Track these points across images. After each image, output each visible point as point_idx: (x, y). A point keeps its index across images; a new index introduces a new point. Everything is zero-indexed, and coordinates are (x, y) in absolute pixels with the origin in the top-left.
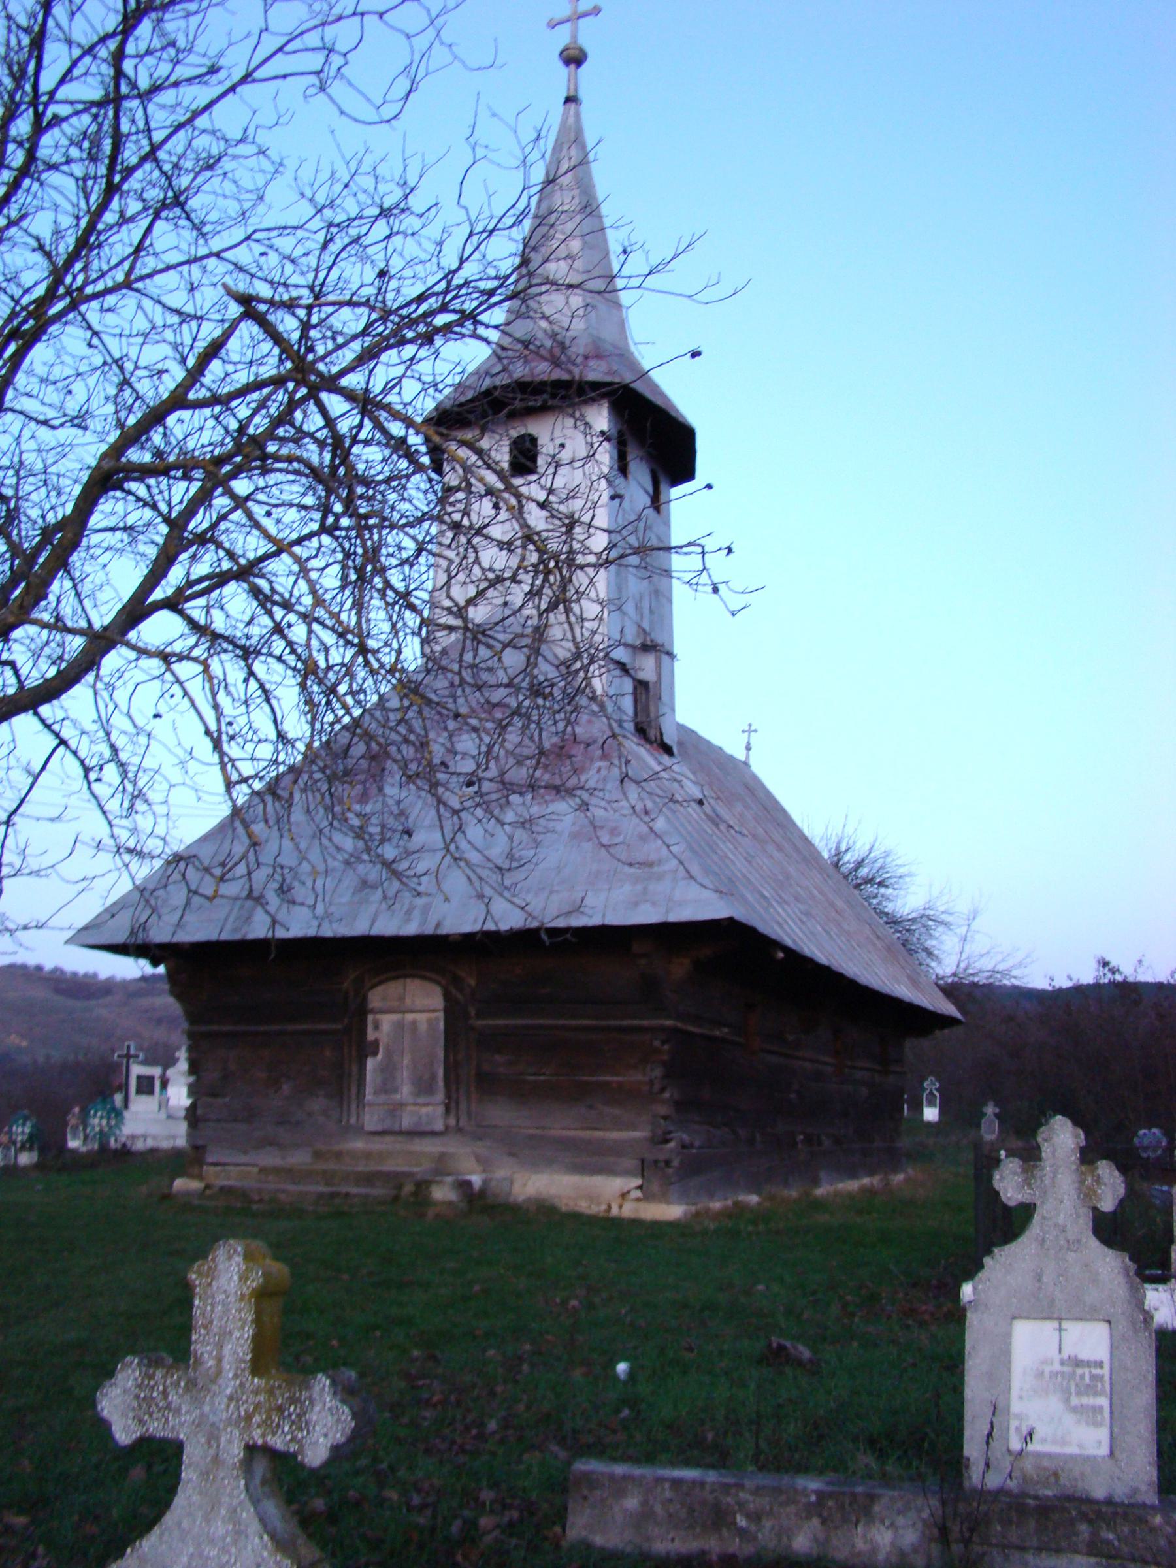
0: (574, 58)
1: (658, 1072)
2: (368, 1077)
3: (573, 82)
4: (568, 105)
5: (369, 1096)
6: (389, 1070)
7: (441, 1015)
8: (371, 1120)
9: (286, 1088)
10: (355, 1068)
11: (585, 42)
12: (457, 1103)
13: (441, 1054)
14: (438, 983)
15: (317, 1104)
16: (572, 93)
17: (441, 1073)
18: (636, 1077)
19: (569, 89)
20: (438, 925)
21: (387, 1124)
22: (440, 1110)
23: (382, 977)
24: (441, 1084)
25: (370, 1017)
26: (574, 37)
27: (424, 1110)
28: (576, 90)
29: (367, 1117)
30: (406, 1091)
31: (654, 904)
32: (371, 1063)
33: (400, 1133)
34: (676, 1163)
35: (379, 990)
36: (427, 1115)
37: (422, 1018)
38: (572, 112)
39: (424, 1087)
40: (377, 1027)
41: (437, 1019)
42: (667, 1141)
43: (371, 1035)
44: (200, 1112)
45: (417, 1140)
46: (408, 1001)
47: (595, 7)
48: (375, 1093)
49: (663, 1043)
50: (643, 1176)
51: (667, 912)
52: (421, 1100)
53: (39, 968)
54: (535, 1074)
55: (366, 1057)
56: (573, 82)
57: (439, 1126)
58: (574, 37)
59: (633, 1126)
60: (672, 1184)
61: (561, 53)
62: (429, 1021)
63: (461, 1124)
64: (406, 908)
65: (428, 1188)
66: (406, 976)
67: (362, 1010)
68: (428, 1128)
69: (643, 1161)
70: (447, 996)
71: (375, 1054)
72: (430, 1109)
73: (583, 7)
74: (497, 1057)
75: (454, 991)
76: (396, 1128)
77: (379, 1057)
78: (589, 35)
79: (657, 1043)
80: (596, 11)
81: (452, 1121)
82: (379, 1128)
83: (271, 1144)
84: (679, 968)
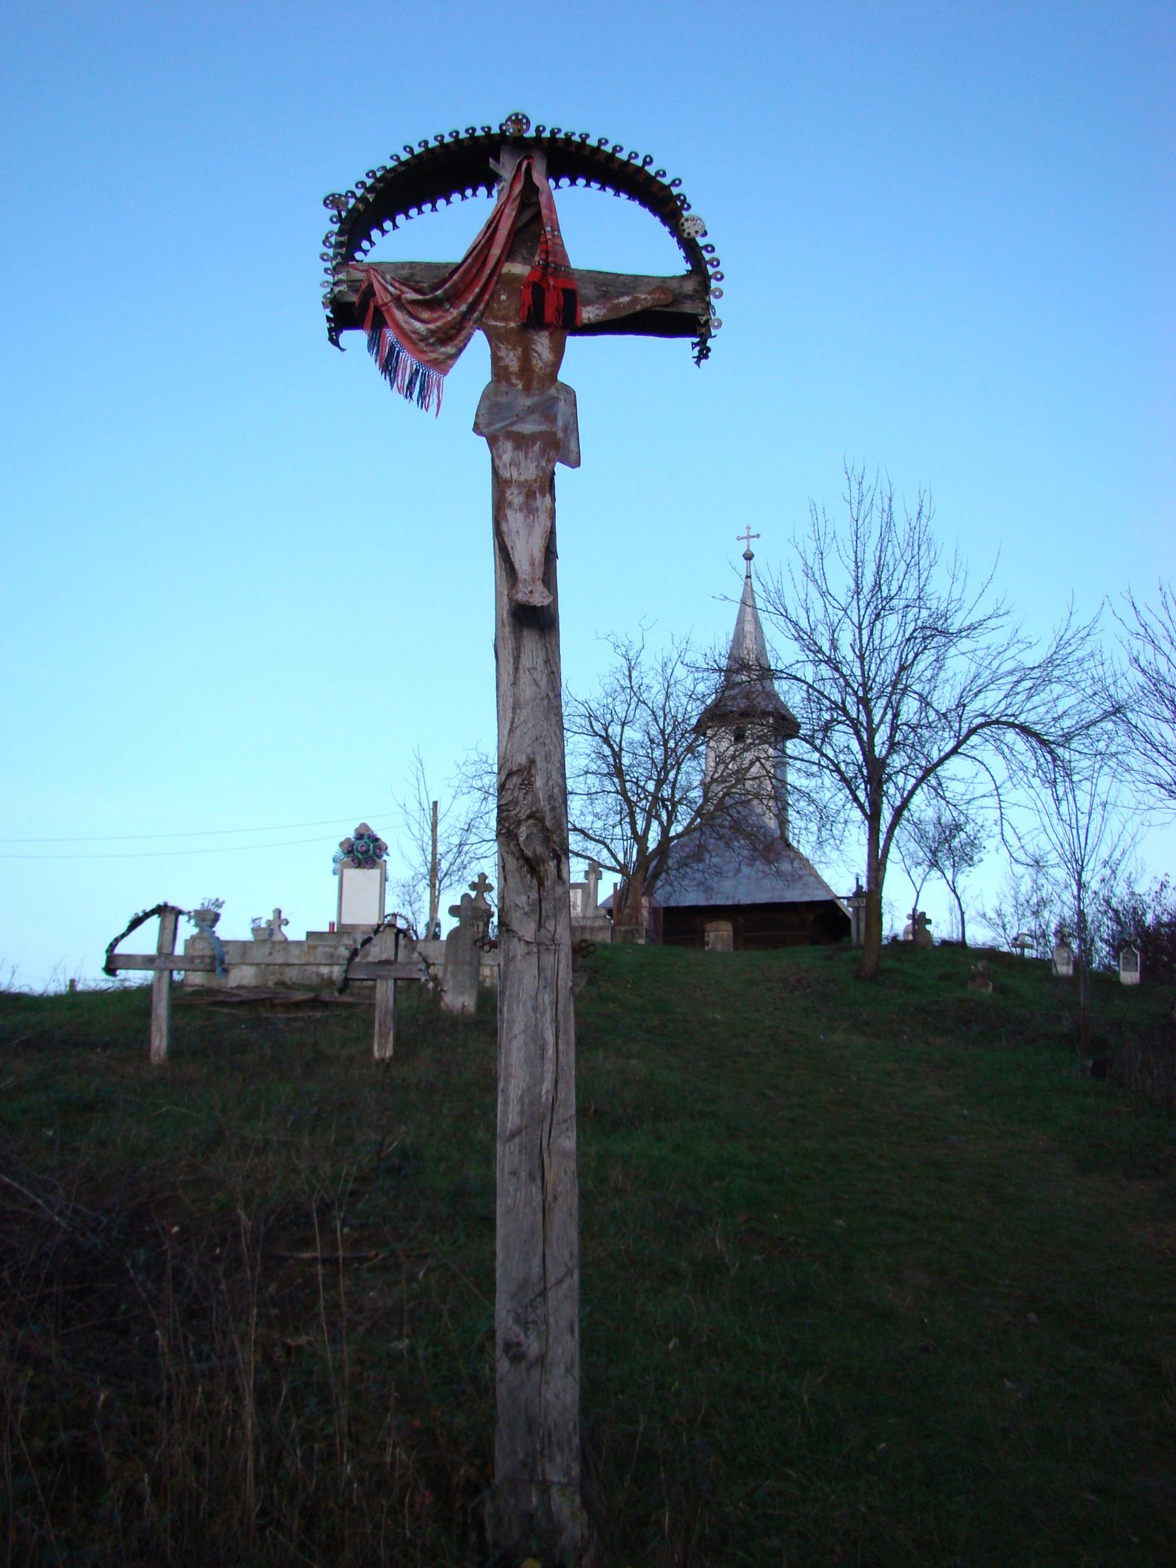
0: (749, 557)
13: (732, 944)
16: (749, 575)
25: (706, 934)
26: (748, 547)
37: (725, 933)
40: (708, 936)
43: (706, 939)
56: (748, 567)
58: (748, 547)
62: (728, 935)
67: (703, 931)
70: (734, 926)
78: (754, 548)
80: (758, 536)
84: (811, 917)
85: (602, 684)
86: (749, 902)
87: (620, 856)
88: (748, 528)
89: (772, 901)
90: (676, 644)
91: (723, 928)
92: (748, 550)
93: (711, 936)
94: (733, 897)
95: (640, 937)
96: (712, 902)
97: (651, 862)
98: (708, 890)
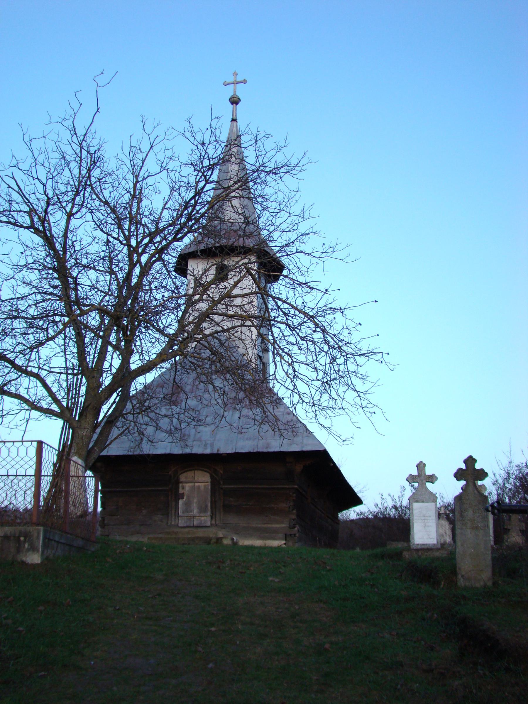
0: (235, 101)
1: (291, 504)
2: (180, 506)
3: (234, 112)
4: (233, 122)
5: (180, 513)
6: (188, 504)
7: (210, 484)
8: (181, 523)
9: (144, 512)
10: (174, 504)
11: (239, 94)
12: (216, 515)
13: (209, 498)
14: (208, 472)
15: (157, 517)
16: (234, 118)
17: (209, 505)
18: (283, 505)
19: (233, 115)
20: (218, 450)
21: (188, 524)
22: (209, 518)
23: (187, 470)
24: (209, 508)
25: (181, 485)
26: (235, 91)
27: (203, 518)
28: (236, 116)
29: (180, 521)
30: (195, 511)
31: (297, 445)
32: (181, 502)
33: (193, 527)
34: (297, 535)
35: (184, 474)
36: (204, 520)
37: (202, 485)
38: (235, 126)
39: (202, 510)
40: (183, 488)
41: (208, 485)
42: (294, 527)
43: (181, 491)
44: (106, 522)
45: (200, 530)
46: (196, 479)
47: (244, 80)
48: (183, 512)
49: (293, 493)
50: (286, 540)
51: (302, 447)
52: (202, 515)
53: (55, 465)
54: (245, 505)
55: (179, 499)
56: (234, 112)
57: (209, 524)
58: (235, 91)
59: (282, 523)
60: (296, 542)
61: (230, 100)
62: (205, 486)
63: (217, 523)
64: (203, 444)
65: (221, 540)
66: (195, 470)
67: (178, 482)
68: (204, 525)
69: (286, 535)
70: (212, 477)
71: (183, 498)
72: (205, 518)
73: (239, 79)
74: (231, 499)
75: (213, 474)
76: (192, 525)
77: (184, 500)
78: (241, 92)
79: (291, 494)
80: (245, 82)
81: (214, 522)
82: (185, 525)
83: (138, 533)
84: (299, 468)
85: (27, 139)
86: (230, 451)
87: (61, 395)
88: (235, 74)
89: (255, 451)
90: (148, 130)
91: (200, 479)
92: (235, 94)
93: (186, 488)
94: (212, 445)
95: (33, 548)
96: (187, 451)
97: (102, 404)
98: (183, 438)
